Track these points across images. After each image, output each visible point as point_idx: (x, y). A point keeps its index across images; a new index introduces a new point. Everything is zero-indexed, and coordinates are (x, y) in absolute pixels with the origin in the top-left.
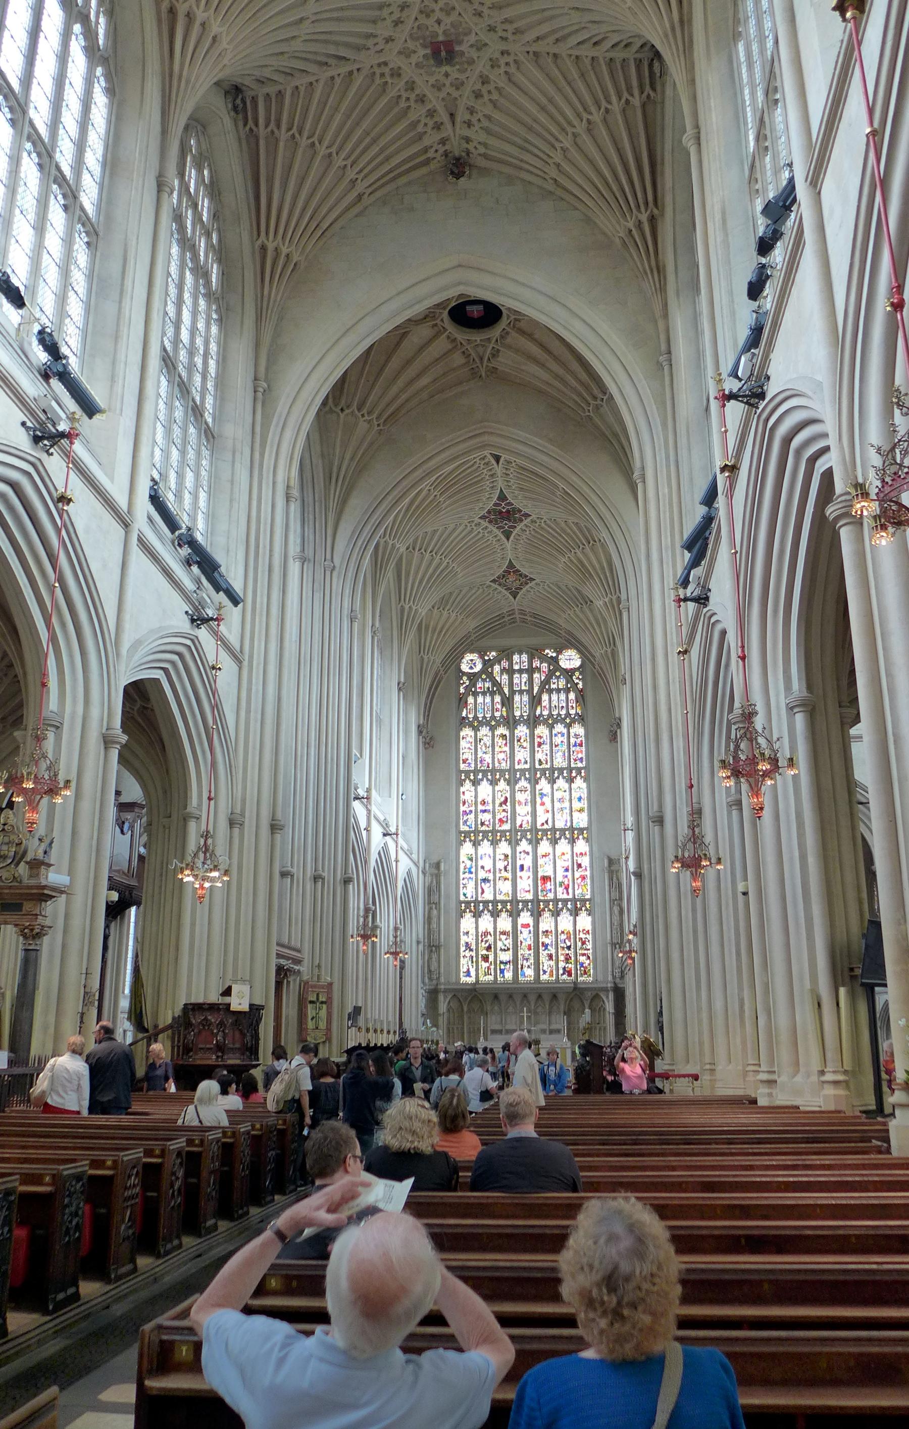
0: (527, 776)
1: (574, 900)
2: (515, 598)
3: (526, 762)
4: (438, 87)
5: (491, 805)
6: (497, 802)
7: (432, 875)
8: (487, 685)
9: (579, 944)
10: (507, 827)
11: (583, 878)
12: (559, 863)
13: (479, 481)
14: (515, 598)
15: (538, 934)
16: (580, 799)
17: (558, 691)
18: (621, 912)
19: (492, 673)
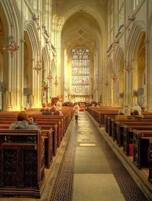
17: (85, 55)
18: (93, 85)
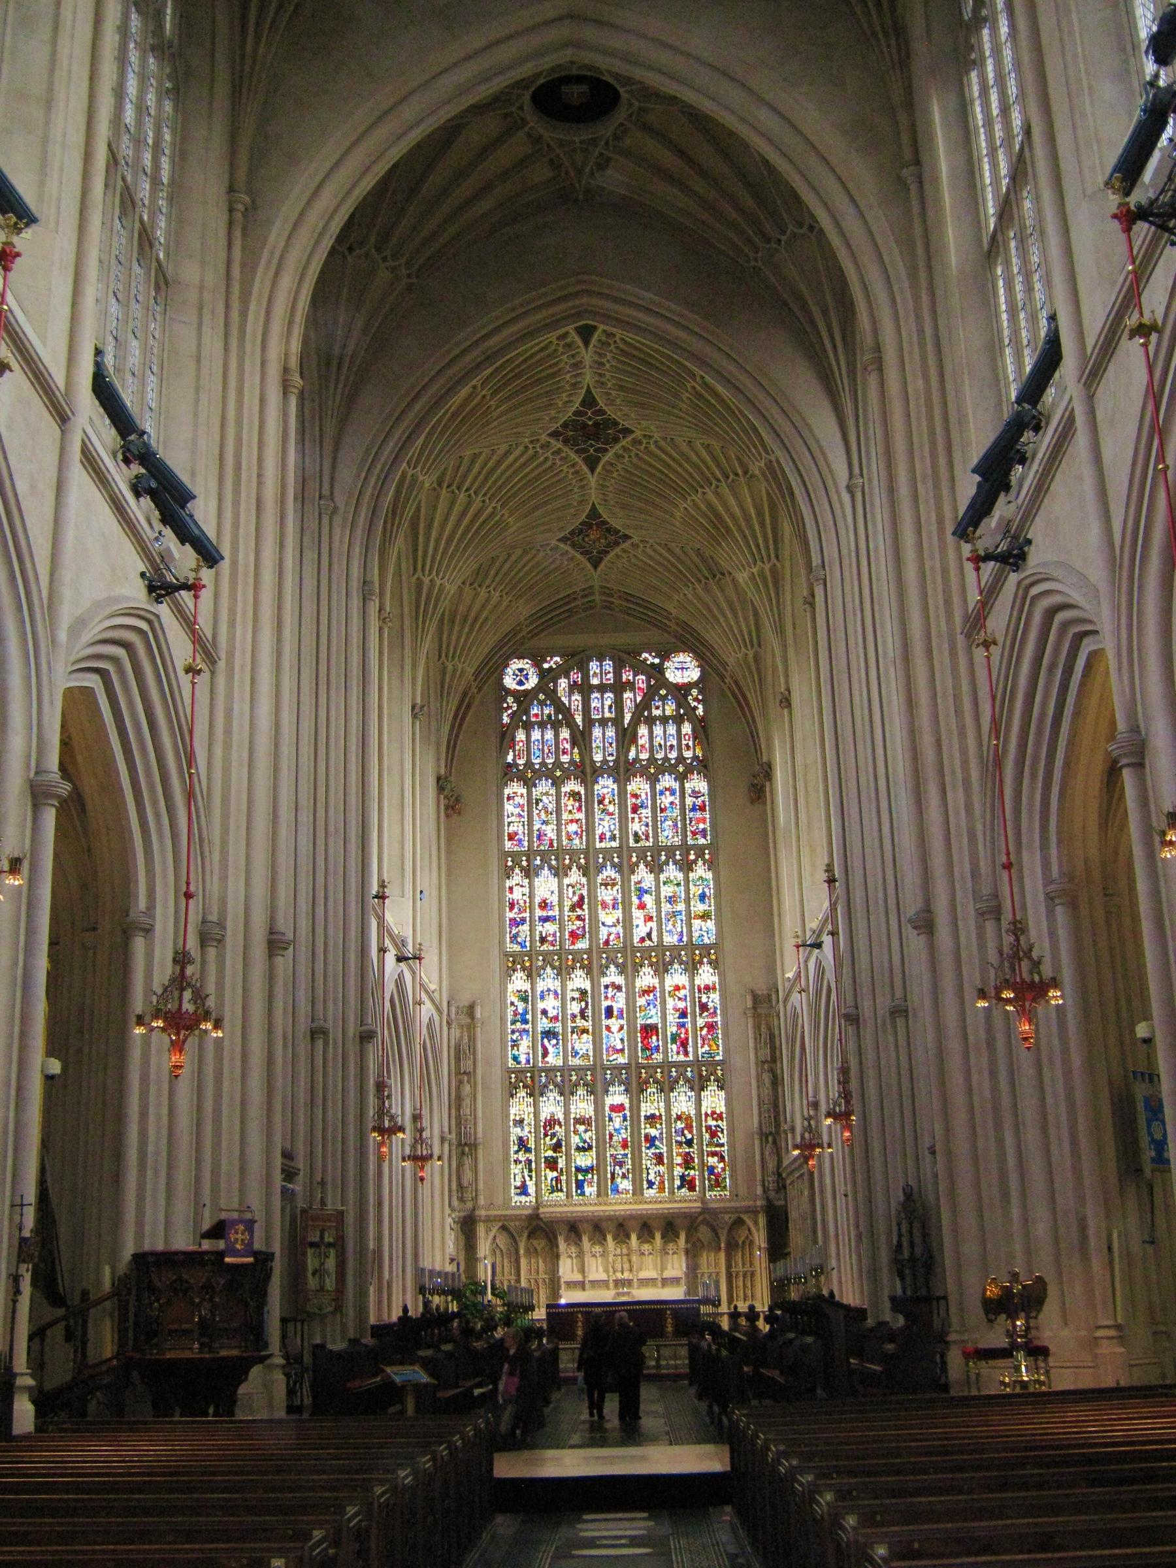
0: (616, 860)
1: (697, 1063)
2: (595, 566)
3: (613, 838)
5: (557, 908)
6: (566, 909)
7: (462, 1027)
8: (546, 712)
9: (707, 1136)
10: (582, 945)
11: (711, 1027)
12: (670, 1003)
13: (554, 375)
14: (596, 566)
15: (639, 1121)
16: (702, 897)
17: (664, 720)
18: (776, 1082)
19: (555, 691)
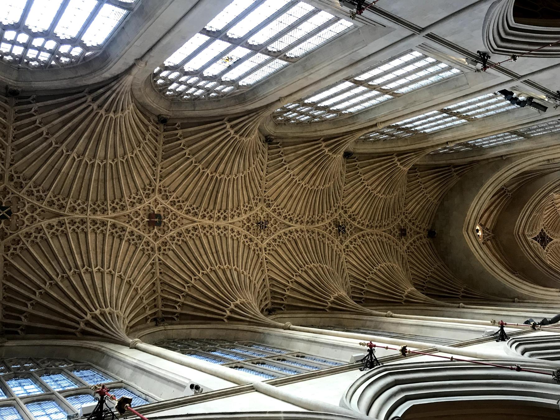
4: (411, 236)
